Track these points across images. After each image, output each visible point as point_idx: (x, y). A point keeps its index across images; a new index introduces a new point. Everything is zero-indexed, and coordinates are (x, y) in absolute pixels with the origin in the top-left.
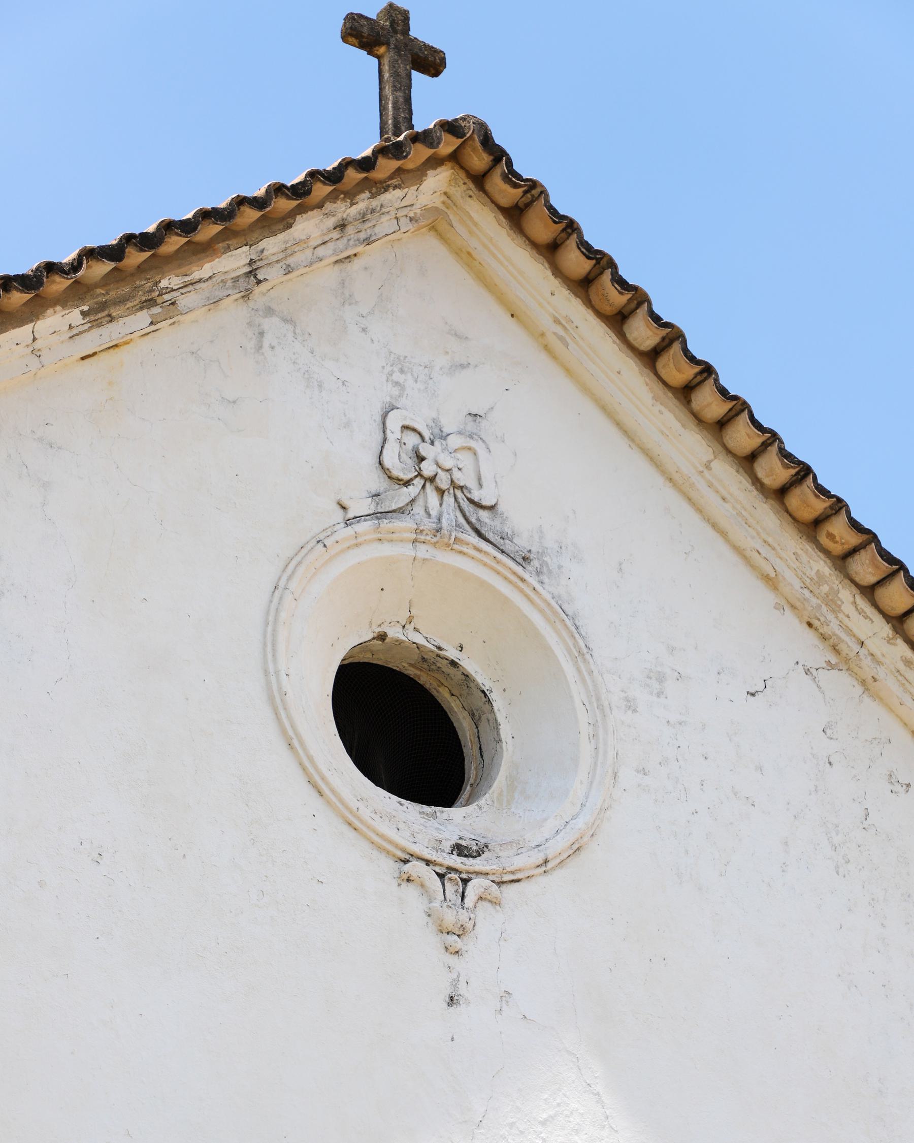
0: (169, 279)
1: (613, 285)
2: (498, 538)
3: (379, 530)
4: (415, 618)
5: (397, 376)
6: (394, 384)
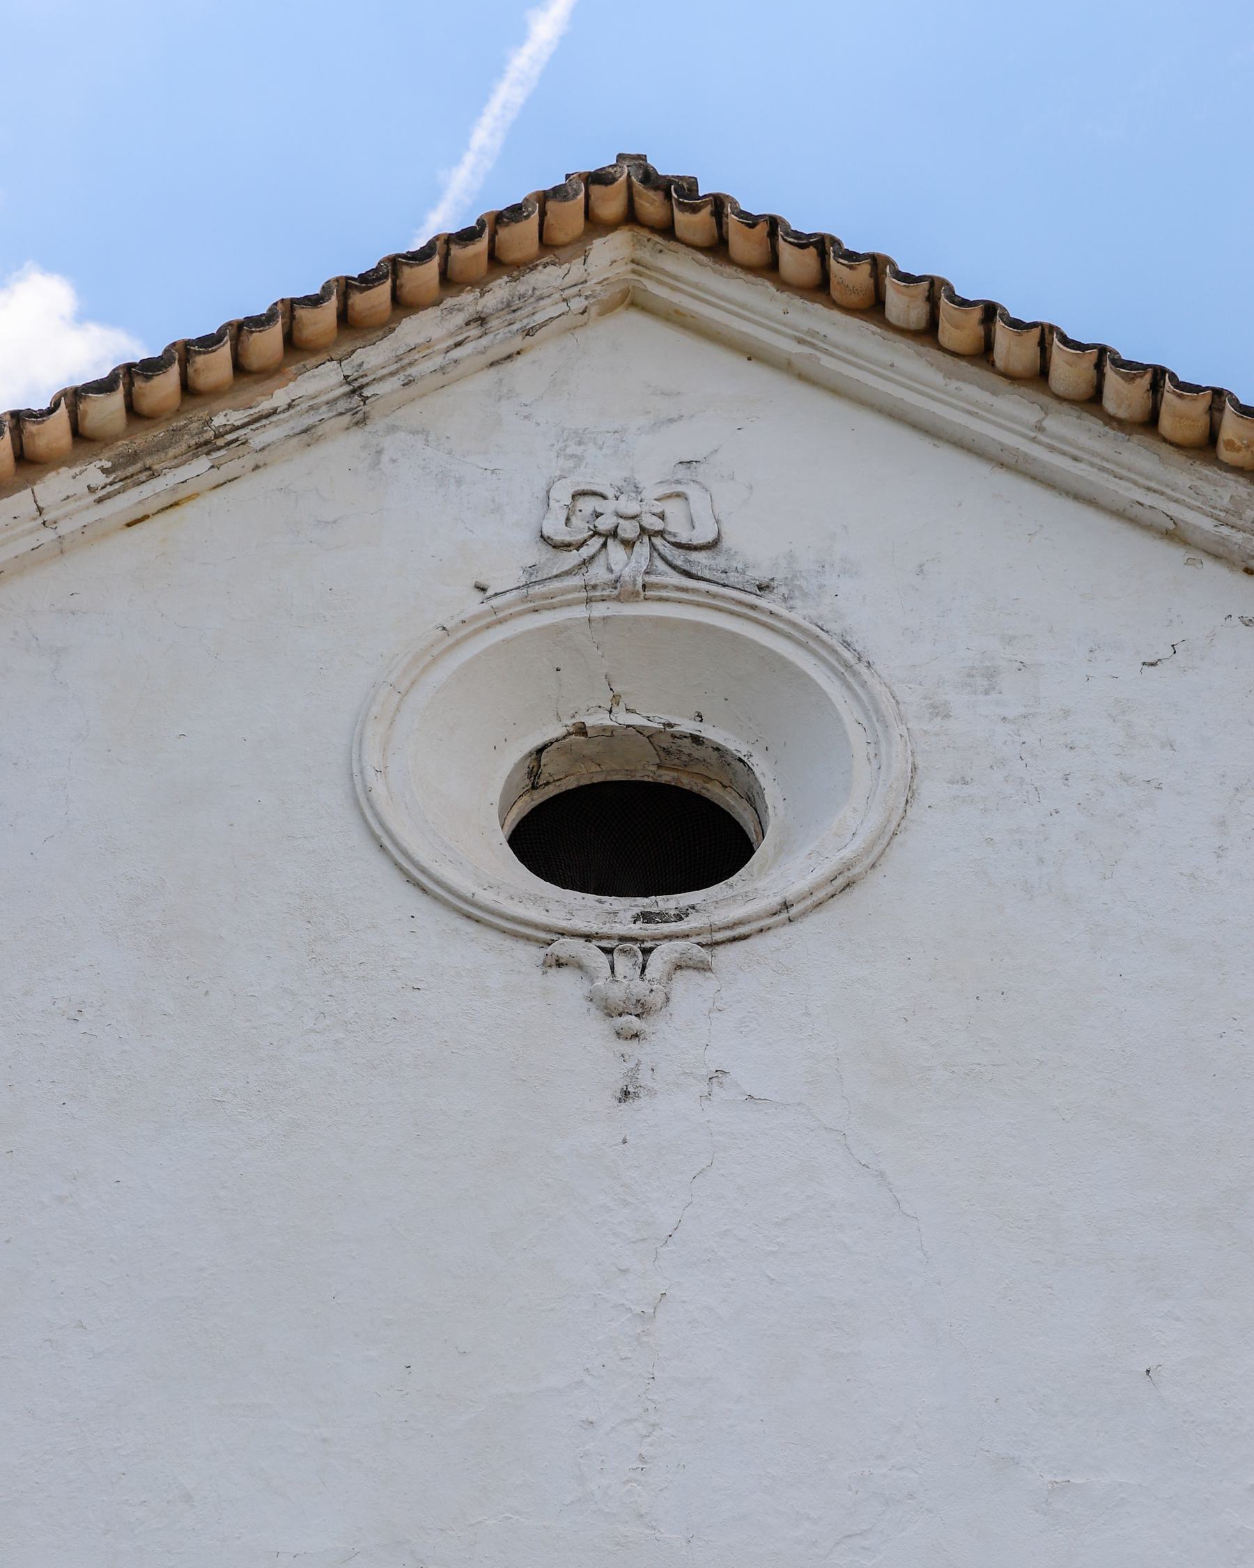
0: (225, 416)
1: (838, 262)
2: (719, 574)
3: (528, 599)
4: (623, 696)
5: (573, 449)
6: (567, 458)
